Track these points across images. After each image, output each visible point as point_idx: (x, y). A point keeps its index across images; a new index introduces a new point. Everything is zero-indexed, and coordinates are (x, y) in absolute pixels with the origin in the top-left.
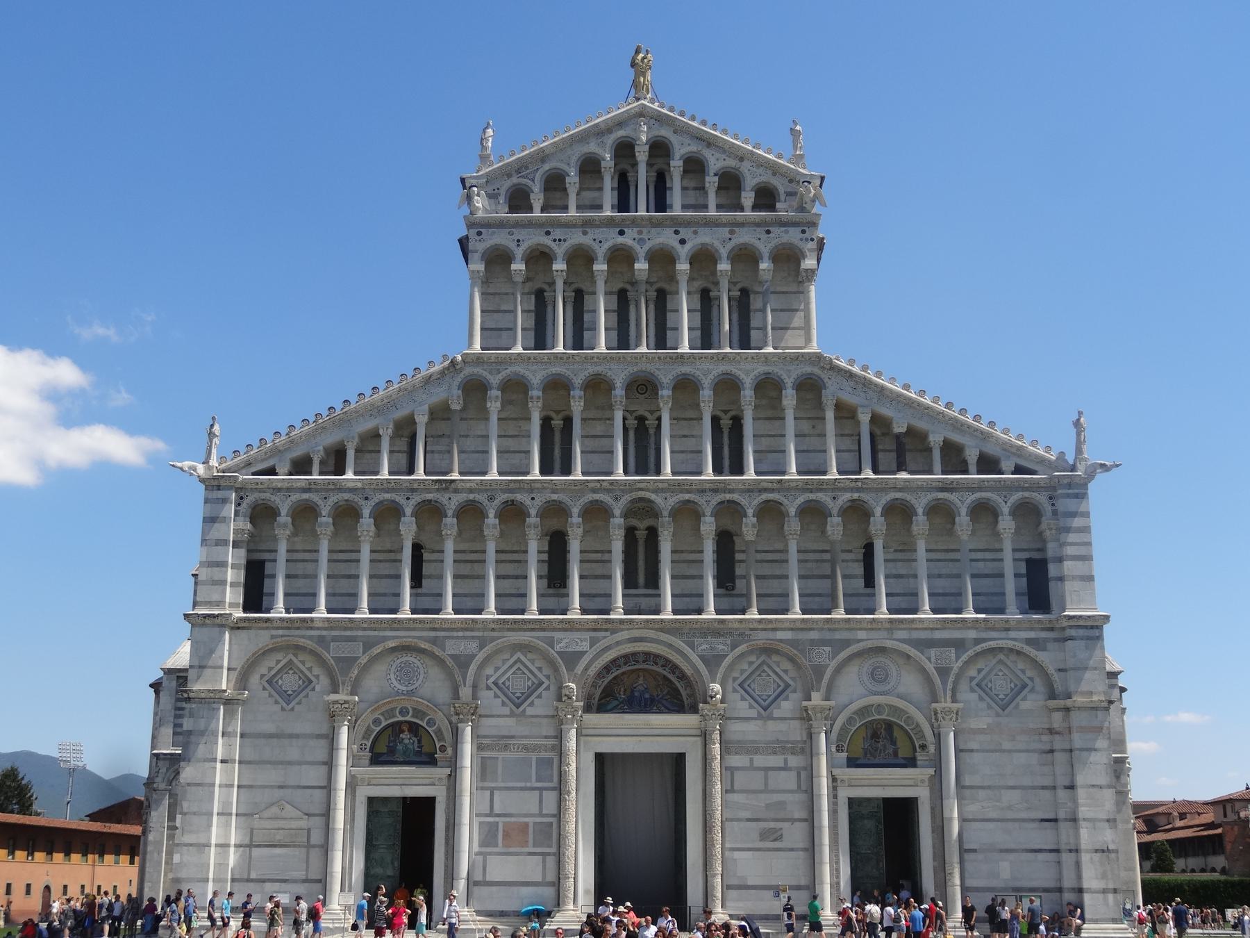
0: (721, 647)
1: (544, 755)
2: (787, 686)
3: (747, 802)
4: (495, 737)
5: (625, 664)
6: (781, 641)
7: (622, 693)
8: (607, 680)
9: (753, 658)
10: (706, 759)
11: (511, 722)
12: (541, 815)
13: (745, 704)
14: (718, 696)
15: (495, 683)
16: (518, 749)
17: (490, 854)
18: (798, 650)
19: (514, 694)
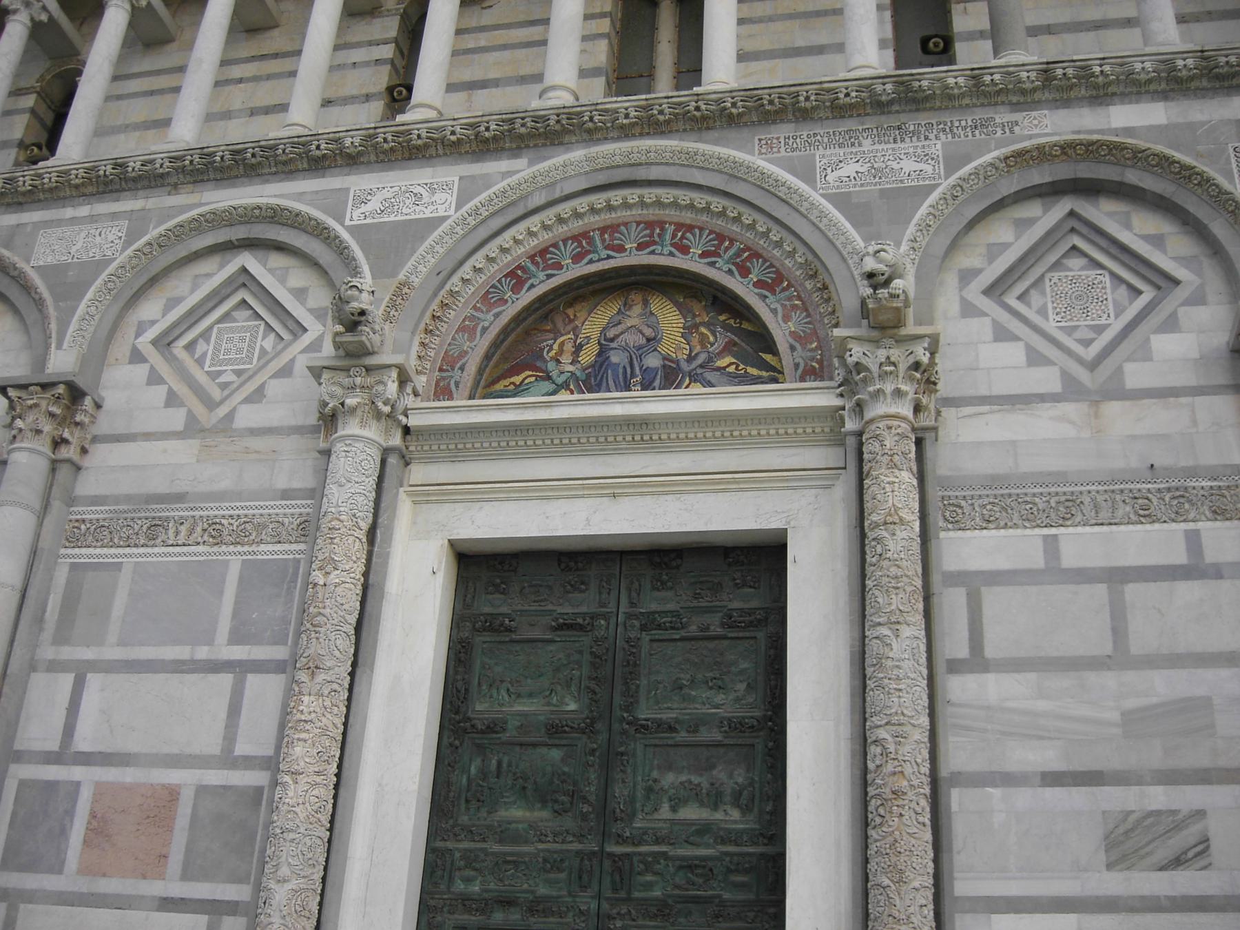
0: (909, 165)
1: (268, 551)
2: (1165, 281)
3: (1042, 705)
4: (129, 498)
5: (577, 258)
6: (1129, 131)
7: (566, 359)
8: (510, 311)
9: (1032, 209)
10: (863, 536)
11: (182, 452)
12: (229, 760)
13: (1014, 353)
14: (897, 283)
15: (164, 342)
16: (191, 532)
17: (31, 897)
18: (1199, 156)
19: (220, 373)
